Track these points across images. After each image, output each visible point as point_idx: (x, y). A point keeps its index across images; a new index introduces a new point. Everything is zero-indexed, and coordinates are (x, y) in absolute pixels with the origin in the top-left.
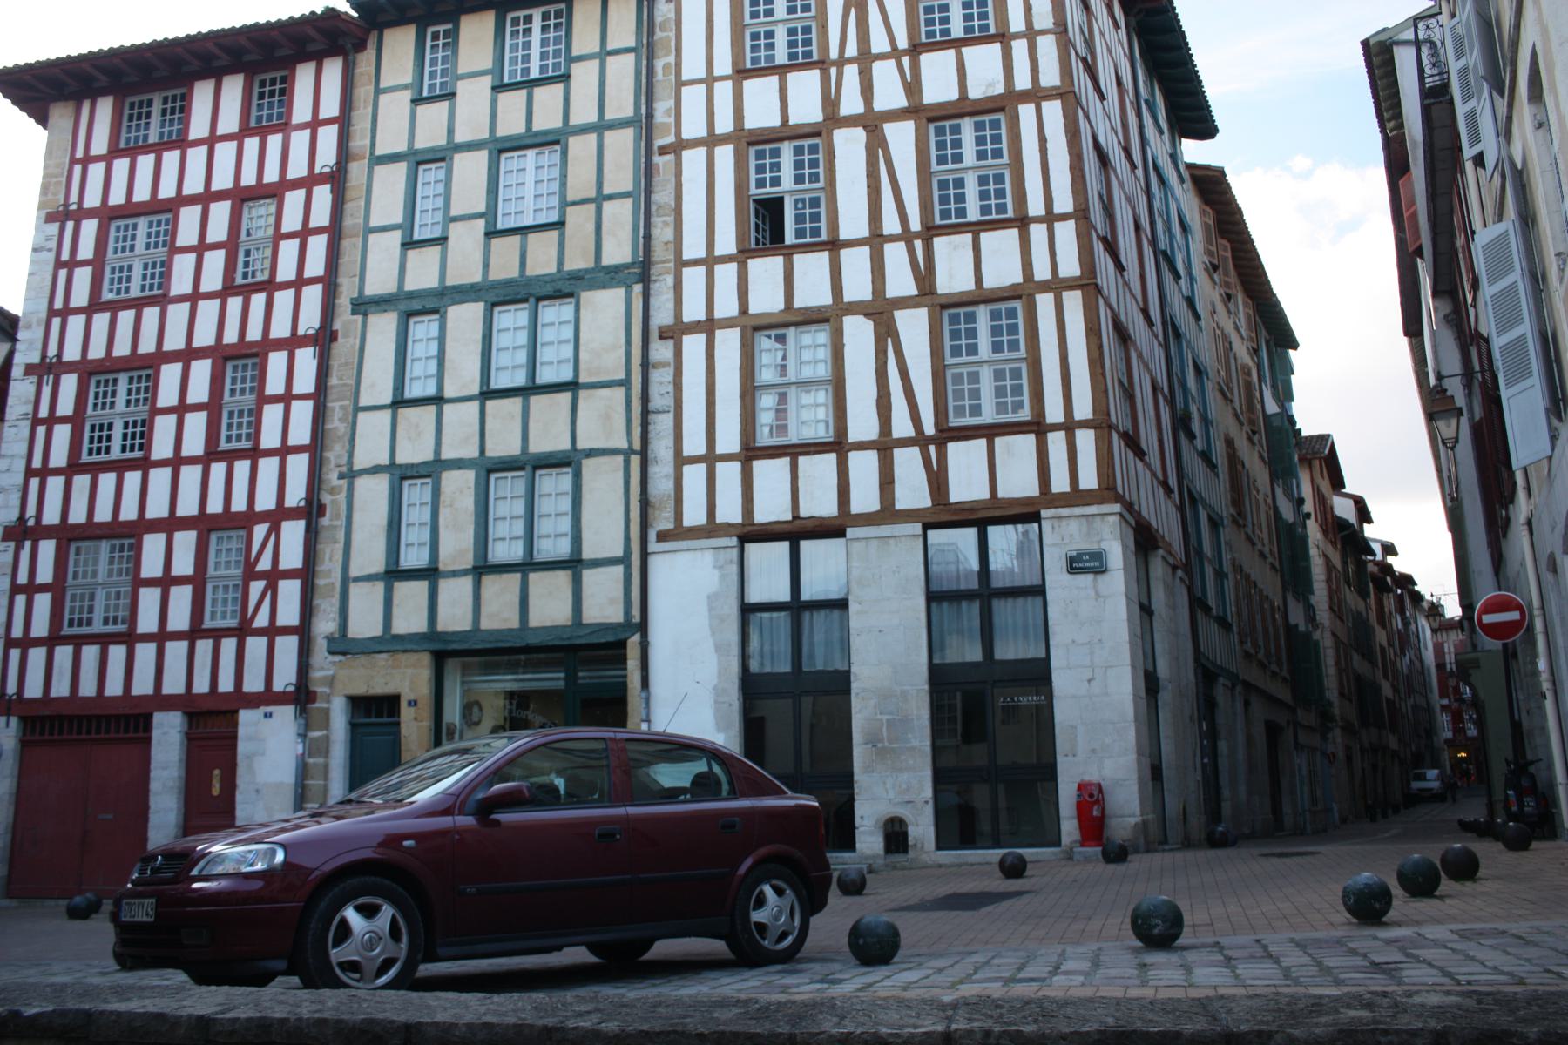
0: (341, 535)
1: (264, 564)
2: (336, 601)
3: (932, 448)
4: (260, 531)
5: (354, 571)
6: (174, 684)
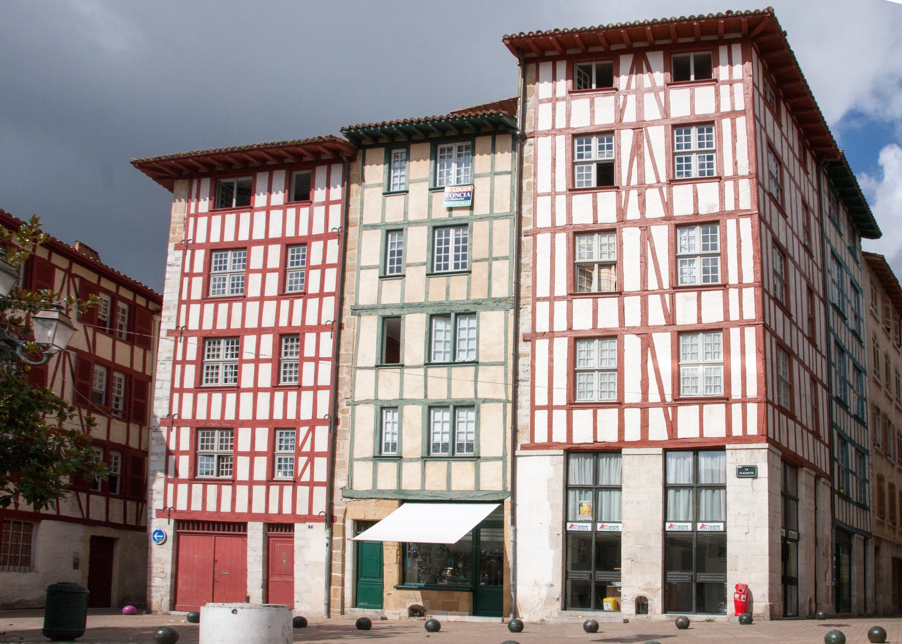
0: (349, 435)
1: (307, 448)
2: (346, 470)
3: (670, 409)
4: (303, 430)
5: (356, 456)
6: (258, 507)
